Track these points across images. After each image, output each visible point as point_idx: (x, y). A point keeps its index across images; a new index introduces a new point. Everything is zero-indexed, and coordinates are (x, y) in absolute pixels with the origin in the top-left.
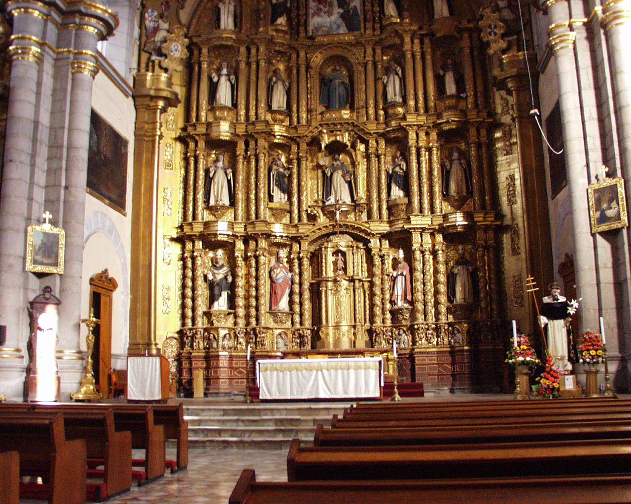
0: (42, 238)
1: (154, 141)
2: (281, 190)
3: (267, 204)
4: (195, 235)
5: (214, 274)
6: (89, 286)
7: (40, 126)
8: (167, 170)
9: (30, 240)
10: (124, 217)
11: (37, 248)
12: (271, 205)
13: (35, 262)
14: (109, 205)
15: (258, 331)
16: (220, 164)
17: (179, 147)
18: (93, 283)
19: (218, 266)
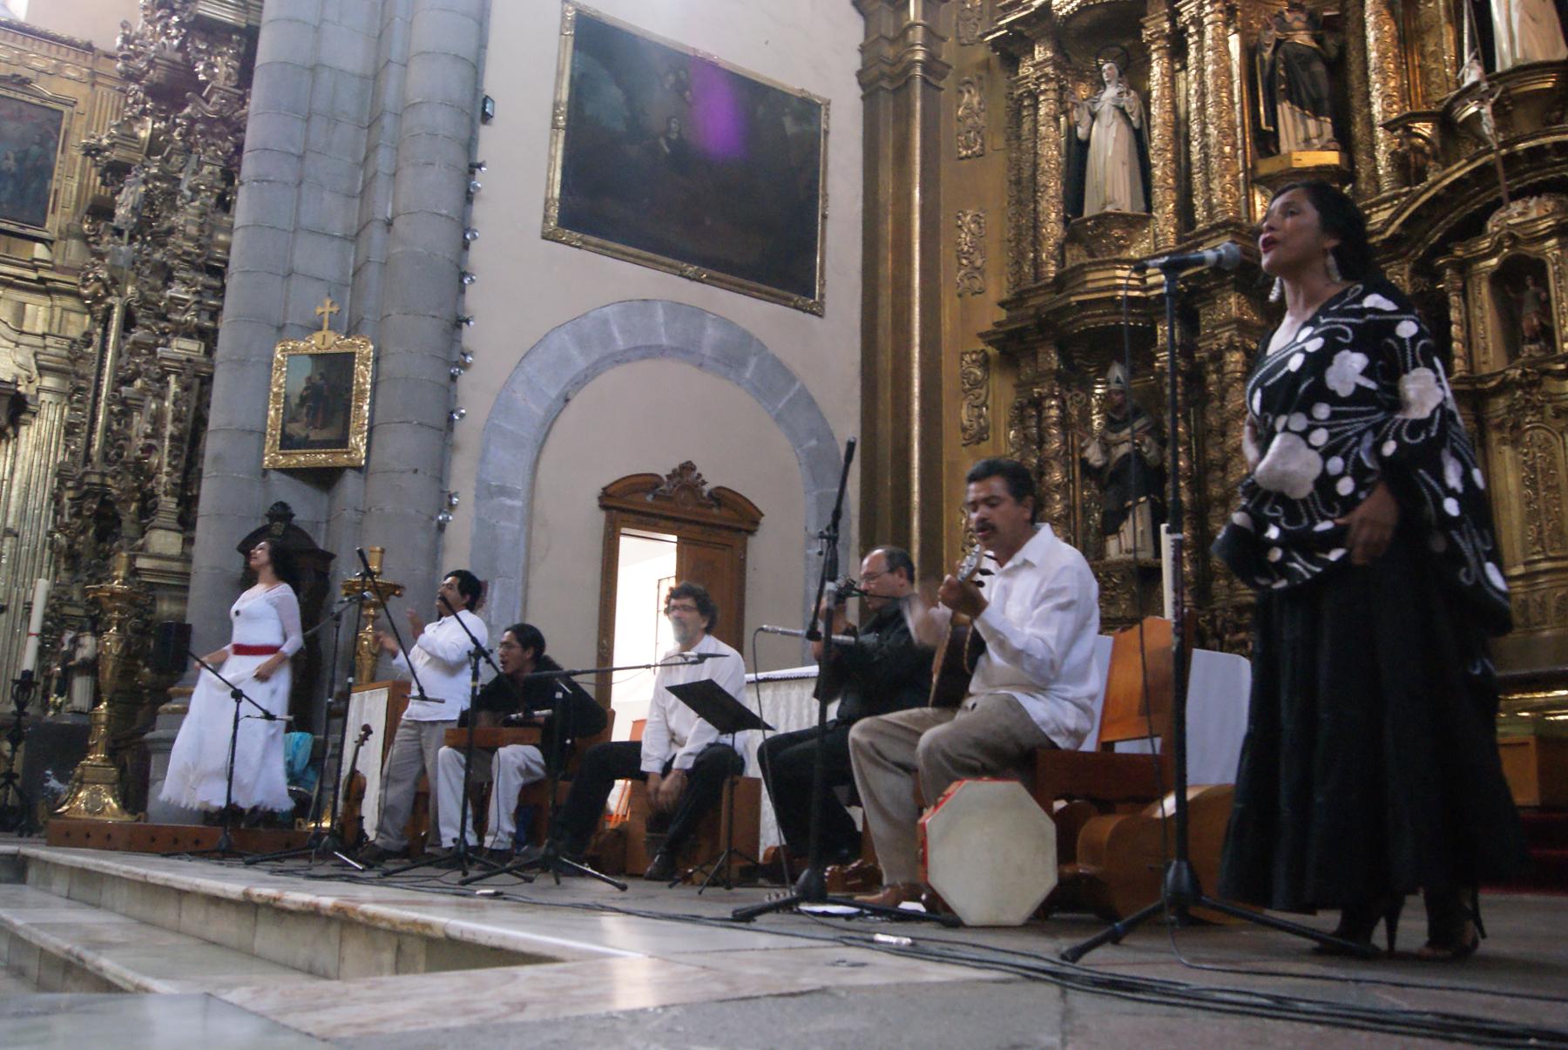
0: (307, 372)
1: (909, 81)
2: (1302, 108)
3: (1254, 167)
4: (1024, 329)
5: (1107, 447)
6: (602, 515)
7: (325, 75)
8: (966, 162)
9: (279, 378)
10: (815, 318)
11: (295, 400)
12: (1267, 167)
13: (287, 442)
14: (711, 281)
15: (1219, 623)
16: (1111, 92)
17: (1002, 79)
18: (608, 502)
19: (1118, 418)
